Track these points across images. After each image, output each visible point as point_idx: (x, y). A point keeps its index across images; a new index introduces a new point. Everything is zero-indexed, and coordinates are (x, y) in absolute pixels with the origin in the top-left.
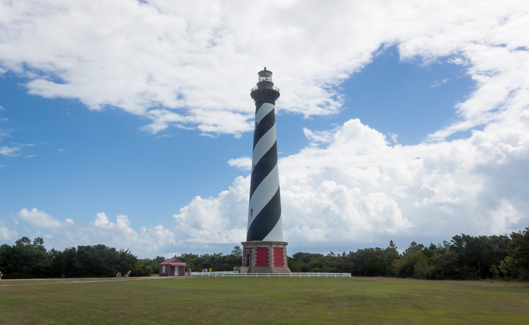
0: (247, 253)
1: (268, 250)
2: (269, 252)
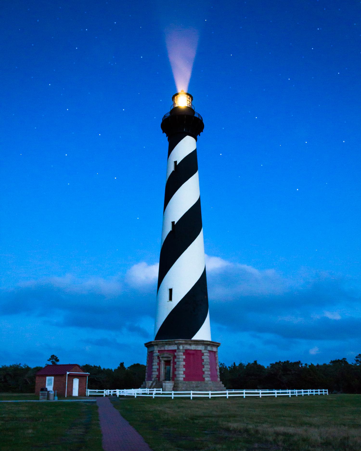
0: (166, 359)
1: (203, 354)
2: (203, 357)
